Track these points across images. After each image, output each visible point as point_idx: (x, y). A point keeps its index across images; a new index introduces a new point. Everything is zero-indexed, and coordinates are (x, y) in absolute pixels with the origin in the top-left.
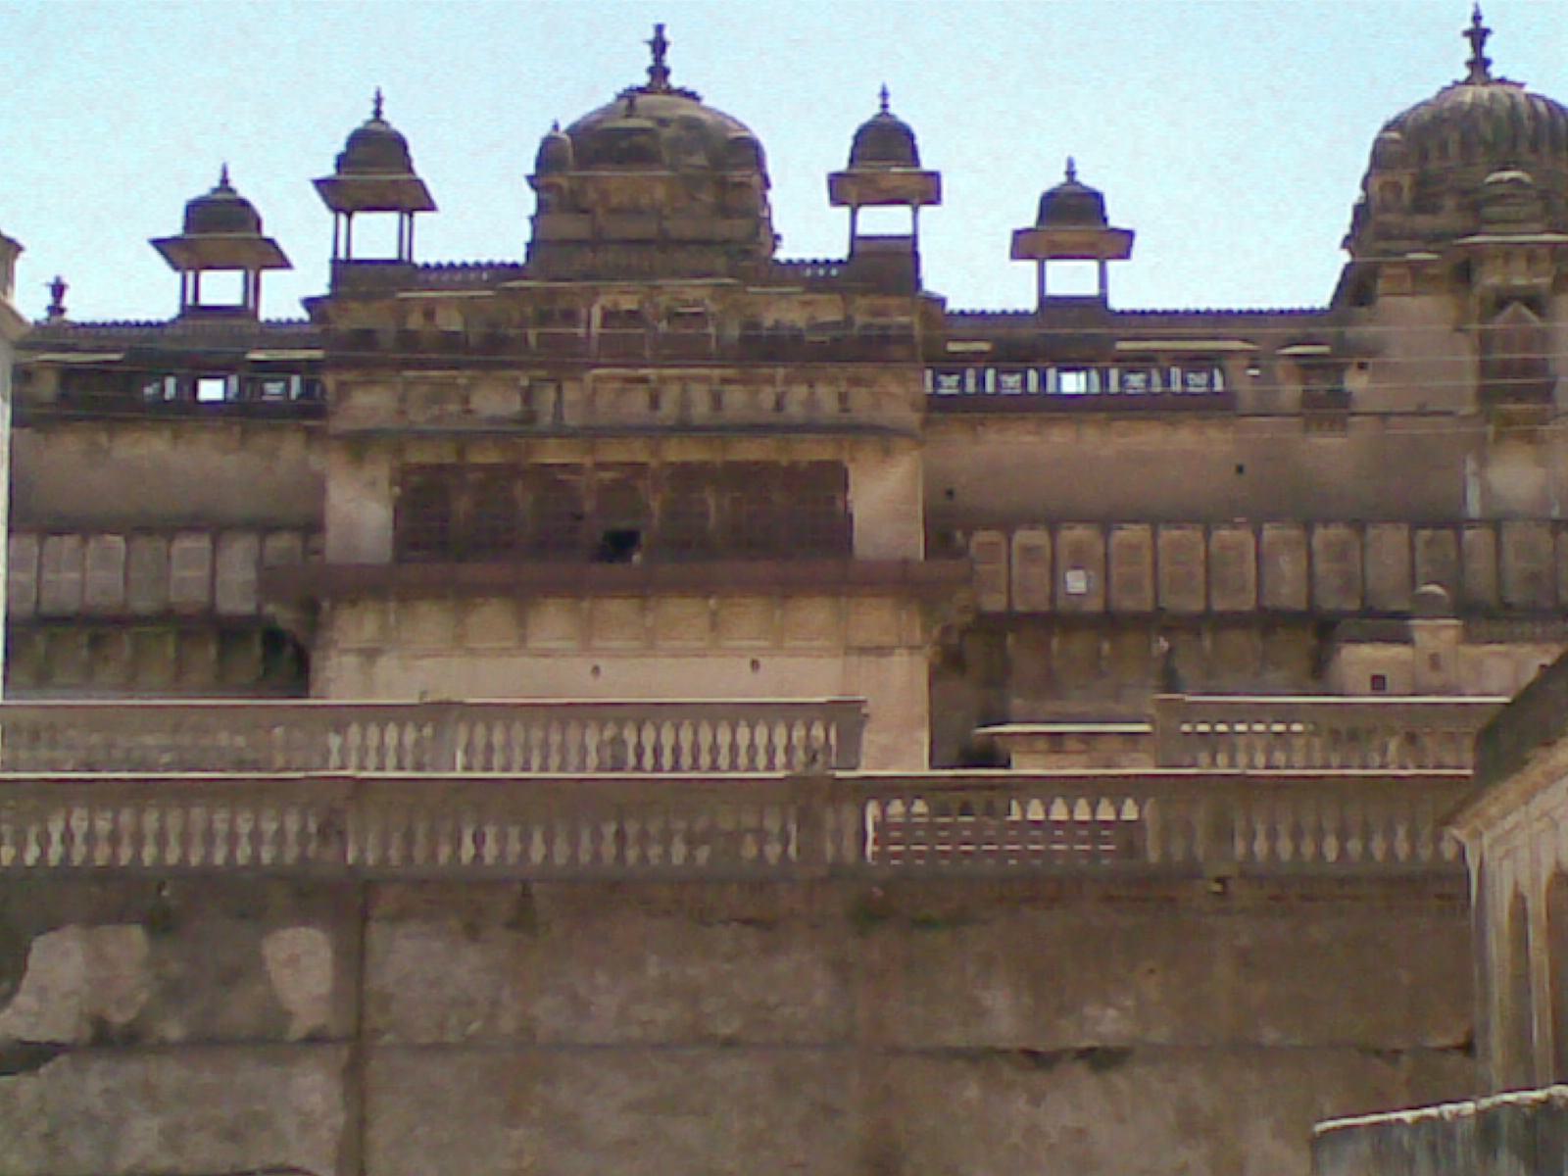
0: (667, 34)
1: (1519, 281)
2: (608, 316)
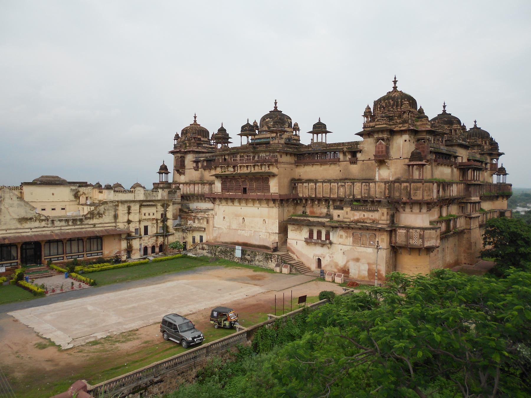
0: (277, 101)
2: (241, 157)
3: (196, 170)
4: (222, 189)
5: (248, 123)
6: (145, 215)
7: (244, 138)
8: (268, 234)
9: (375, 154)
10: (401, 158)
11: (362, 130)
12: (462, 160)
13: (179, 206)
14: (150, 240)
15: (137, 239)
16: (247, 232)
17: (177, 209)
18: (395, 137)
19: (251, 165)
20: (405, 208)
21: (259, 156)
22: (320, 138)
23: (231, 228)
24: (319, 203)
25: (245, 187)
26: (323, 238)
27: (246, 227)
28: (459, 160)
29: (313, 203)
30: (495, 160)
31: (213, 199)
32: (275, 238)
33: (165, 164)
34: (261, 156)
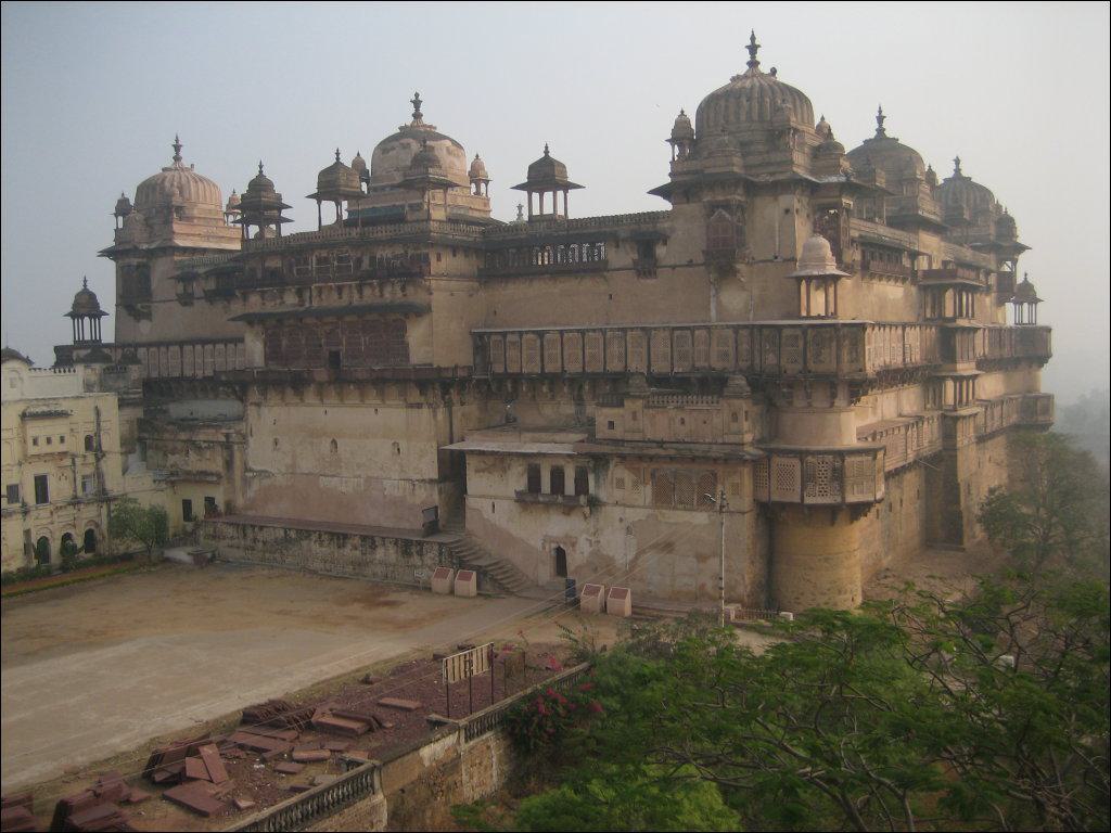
1: (720, 198)
2: (319, 261)
3: (185, 304)
4: (268, 357)
5: (338, 163)
6: (35, 442)
7: (329, 208)
8: (408, 485)
9: (705, 248)
10: (776, 258)
11: (669, 180)
12: (930, 264)
13: (139, 413)
14: (55, 516)
15: (14, 517)
16: (346, 482)
17: (132, 422)
18: (758, 201)
19: (350, 286)
20: (792, 397)
21: (373, 259)
22: (548, 203)
23: (298, 471)
24: (551, 390)
25: (334, 349)
26: (570, 488)
27: (341, 467)
28: (923, 264)
29: (534, 390)
30: (1009, 263)
31: (239, 385)
32: (431, 496)
33: (91, 288)
34: (382, 258)
